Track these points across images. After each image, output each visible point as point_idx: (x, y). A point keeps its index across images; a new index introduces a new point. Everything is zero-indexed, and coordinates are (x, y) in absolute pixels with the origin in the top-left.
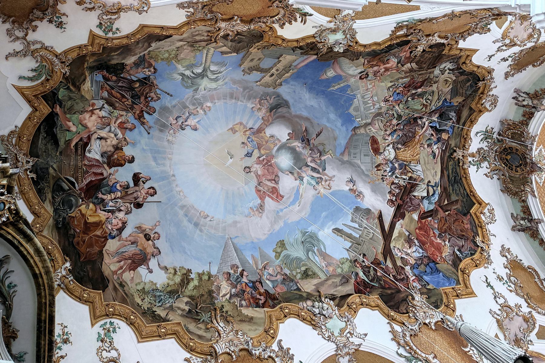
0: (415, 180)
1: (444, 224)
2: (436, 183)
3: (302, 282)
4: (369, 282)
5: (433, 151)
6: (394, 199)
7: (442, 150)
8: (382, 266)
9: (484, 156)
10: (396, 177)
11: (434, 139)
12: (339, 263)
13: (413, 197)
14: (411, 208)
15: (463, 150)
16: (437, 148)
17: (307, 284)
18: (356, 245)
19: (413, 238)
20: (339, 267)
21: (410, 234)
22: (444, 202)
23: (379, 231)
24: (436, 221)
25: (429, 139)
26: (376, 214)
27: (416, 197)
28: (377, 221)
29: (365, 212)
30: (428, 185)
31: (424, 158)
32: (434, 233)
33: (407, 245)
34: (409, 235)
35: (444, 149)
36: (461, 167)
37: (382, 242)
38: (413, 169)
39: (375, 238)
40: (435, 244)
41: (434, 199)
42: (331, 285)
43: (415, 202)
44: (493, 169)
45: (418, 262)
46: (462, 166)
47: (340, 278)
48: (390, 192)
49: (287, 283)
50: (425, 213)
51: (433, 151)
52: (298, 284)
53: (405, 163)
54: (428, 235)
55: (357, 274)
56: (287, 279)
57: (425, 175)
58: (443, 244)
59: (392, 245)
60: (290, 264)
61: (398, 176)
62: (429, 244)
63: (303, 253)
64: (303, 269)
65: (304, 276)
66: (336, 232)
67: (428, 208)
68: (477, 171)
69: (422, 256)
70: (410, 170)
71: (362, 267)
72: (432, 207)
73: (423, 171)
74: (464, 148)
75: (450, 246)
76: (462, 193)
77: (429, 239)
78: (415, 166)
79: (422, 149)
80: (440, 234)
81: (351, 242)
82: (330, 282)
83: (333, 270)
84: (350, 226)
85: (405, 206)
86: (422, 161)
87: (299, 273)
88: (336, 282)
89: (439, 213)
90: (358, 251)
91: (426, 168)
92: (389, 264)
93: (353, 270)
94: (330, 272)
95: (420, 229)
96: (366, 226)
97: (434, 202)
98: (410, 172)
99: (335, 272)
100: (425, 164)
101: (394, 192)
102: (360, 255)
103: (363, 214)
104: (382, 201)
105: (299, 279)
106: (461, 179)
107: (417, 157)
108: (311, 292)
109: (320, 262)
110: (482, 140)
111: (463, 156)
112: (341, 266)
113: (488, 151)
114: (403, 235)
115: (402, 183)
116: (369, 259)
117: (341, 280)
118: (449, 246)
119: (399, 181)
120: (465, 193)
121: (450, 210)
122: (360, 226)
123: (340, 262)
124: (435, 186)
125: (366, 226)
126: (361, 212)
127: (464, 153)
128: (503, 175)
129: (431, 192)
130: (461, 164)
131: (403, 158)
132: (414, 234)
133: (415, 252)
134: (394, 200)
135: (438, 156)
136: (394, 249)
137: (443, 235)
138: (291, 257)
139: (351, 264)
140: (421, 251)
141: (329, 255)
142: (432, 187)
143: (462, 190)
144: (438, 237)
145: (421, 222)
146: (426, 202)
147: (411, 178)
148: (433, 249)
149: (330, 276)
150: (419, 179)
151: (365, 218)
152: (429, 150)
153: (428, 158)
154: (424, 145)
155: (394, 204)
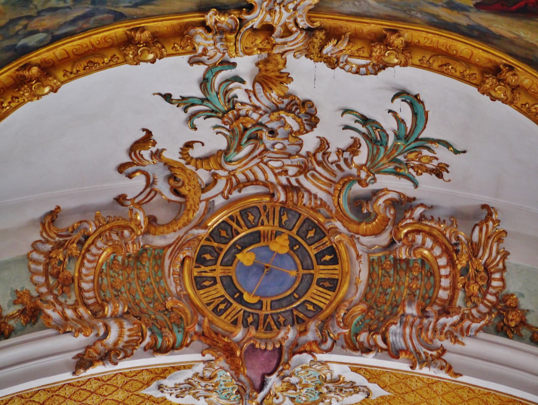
9: (265, 136)
15: (310, 32)
36: (197, 18)
44: (181, 176)
46: (203, 24)
68: (167, 97)
74: (321, 35)
76: (34, 24)
106: (119, 17)
110: (365, 120)
111: (268, 29)
113: (291, 149)
120: (31, 41)
127: (288, 32)
128: (152, 220)
130: (211, 18)
143: (47, 22)
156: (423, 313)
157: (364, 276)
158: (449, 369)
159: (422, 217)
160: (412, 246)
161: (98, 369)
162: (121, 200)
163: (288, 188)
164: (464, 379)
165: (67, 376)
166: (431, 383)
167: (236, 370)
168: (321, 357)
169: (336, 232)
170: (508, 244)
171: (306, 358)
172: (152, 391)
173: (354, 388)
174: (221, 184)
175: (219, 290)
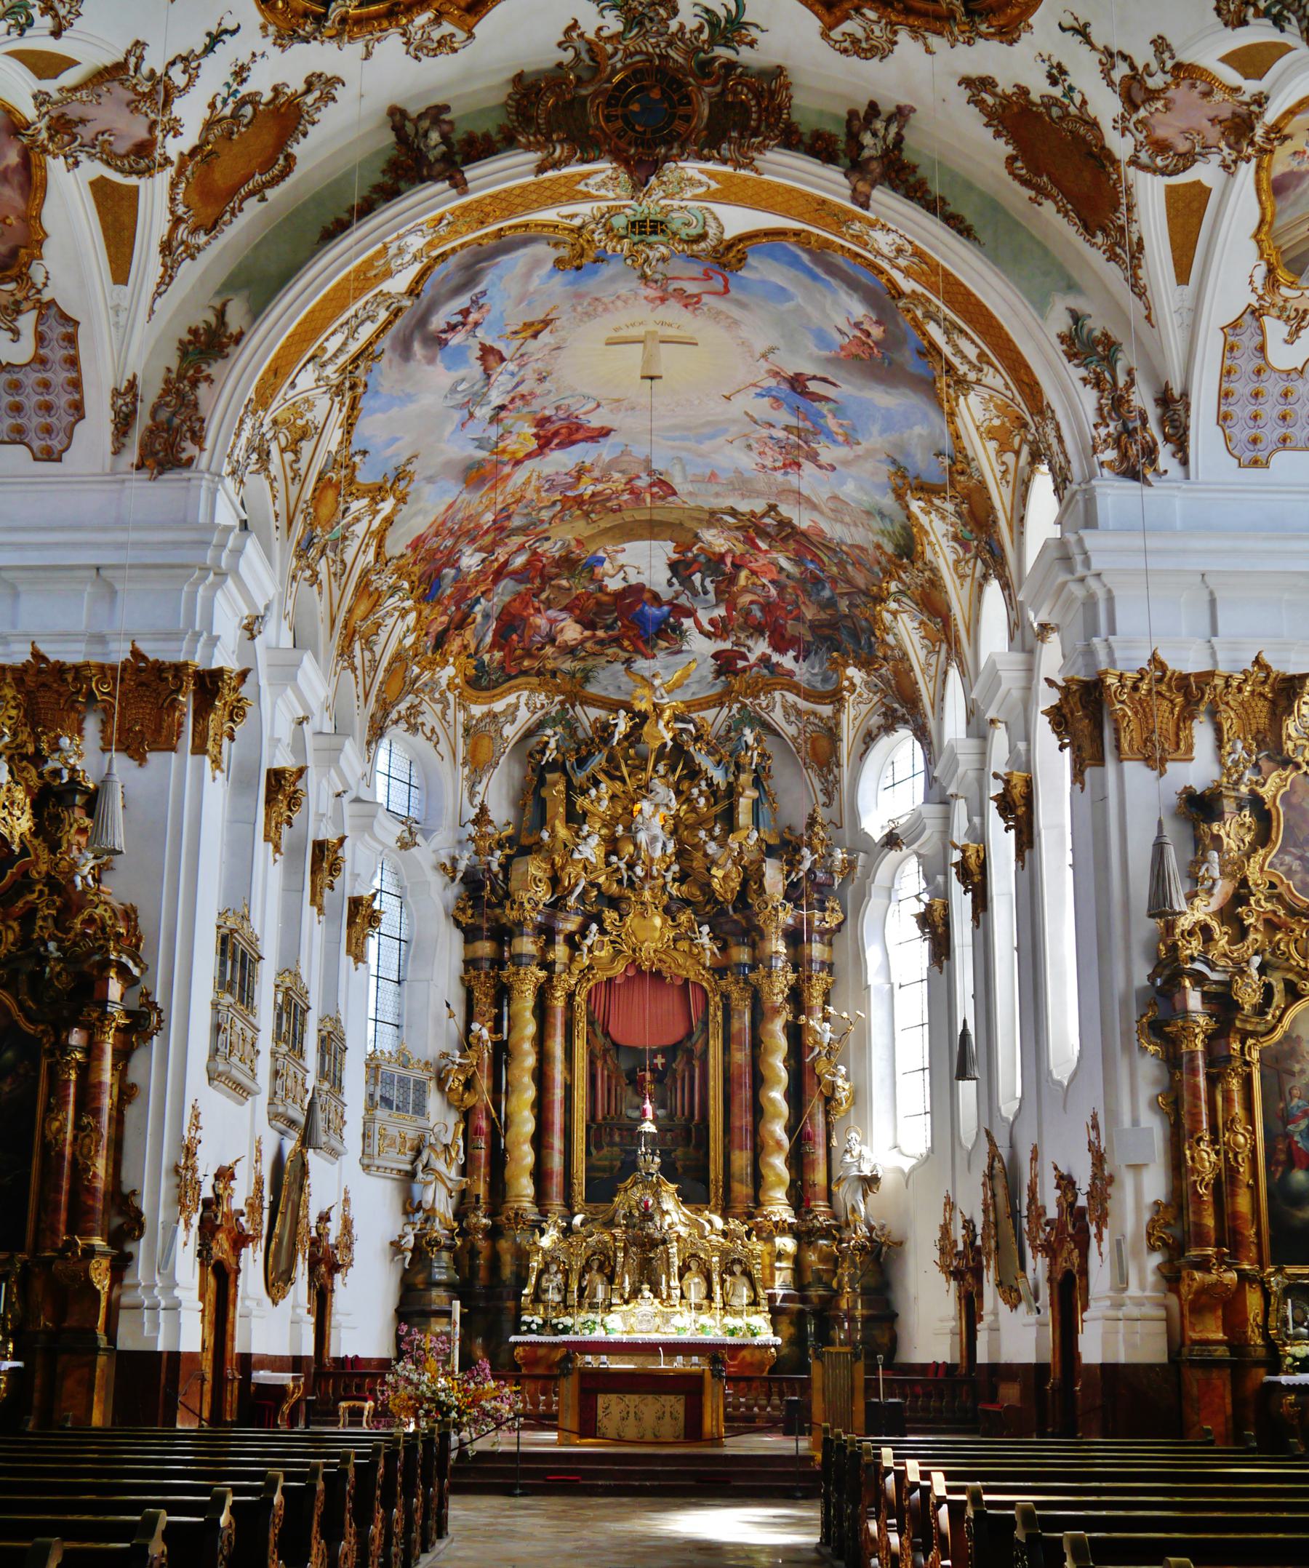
156: (742, 136)
157: (706, 113)
158: (756, 170)
159: (742, 74)
160: (736, 94)
161: (550, 174)
162: (560, 65)
163: (661, 56)
164: (766, 177)
165: (532, 178)
166: (745, 180)
167: (631, 174)
168: (681, 164)
169: (689, 84)
170: (793, 90)
171: (672, 165)
172: (581, 187)
173: (700, 184)
174: (620, 54)
175: (620, 124)
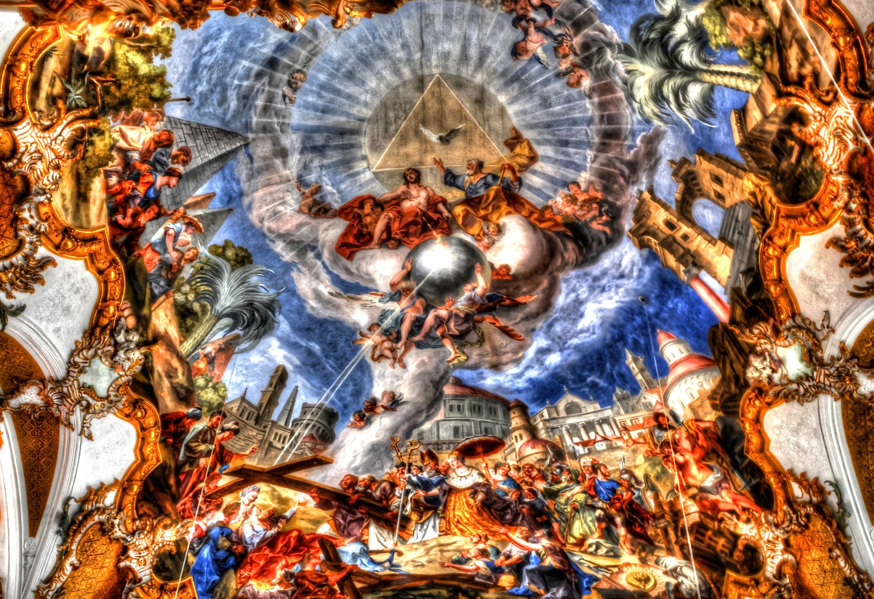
0: (403, 528)
1: (314, 583)
2: (399, 566)
3: (169, 306)
4: (185, 442)
5: (469, 559)
6: (361, 489)
7: (473, 577)
8: (219, 466)
10: (407, 492)
11: (499, 561)
12: (215, 380)
13: (365, 524)
14: (342, 521)
16: (478, 568)
17: (166, 316)
18: (255, 415)
19: (280, 525)
20: (208, 381)
21: (288, 520)
22: (360, 582)
23: (289, 459)
24: (317, 567)
25: (498, 553)
26: (326, 454)
27: (366, 531)
28: (309, 455)
29: (326, 431)
30: (392, 552)
31: (454, 543)
32: (293, 564)
33: (264, 513)
34: (284, 517)
35: (477, 579)
37: (266, 466)
38: (427, 523)
39: (273, 453)
40: (273, 566)
41: (362, 563)
42: (170, 365)
43: (357, 532)
45: (234, 536)
47: (186, 384)
48: (373, 480)
49: (163, 273)
50: (334, 547)
51: (469, 559)
52: (163, 297)
53: (441, 508)
54: (287, 554)
55: (197, 418)
56: (171, 271)
57: (415, 546)
58: (274, 581)
59: (263, 486)
60: (203, 280)
61: (411, 495)
62: (271, 555)
63: (228, 304)
64: (196, 307)
65: (182, 310)
66: (279, 373)
67: (344, 552)
69: (246, 543)
70: (424, 518)
71: (212, 428)
72: (347, 560)
73: (423, 543)
75: (270, 594)
77: (280, 555)
78: (434, 527)
79: (475, 539)
80: (292, 575)
81: (261, 405)
82: (175, 363)
83: (199, 370)
84: (293, 402)
85: (344, 509)
86: (444, 540)
87: (187, 299)
88: (177, 377)
89: (333, 573)
90: (244, 418)
91: (432, 548)
92: (224, 481)
93: (205, 409)
94: (195, 364)
95: (300, 538)
96: (296, 433)
97: (358, 563)
98: (421, 517)
99: (196, 374)
100: (441, 545)
101: (374, 488)
102: (237, 424)
103: (322, 428)
104: (353, 466)
105: (175, 300)
107: (456, 530)
108: (152, 326)
109: (213, 343)
112: (210, 384)
114: (283, 507)
115: (396, 502)
116: (230, 442)
117: (182, 386)
118: (272, 591)
119: (399, 498)
121: (342, 593)
122: (296, 423)
123: (217, 383)
124: (392, 565)
125: (296, 433)
126: (325, 423)
129: (377, 558)
131: (452, 504)
132: (288, 528)
133: (253, 529)
134: (357, 488)
135: (459, 569)
136: (254, 490)
137: (292, 581)
138: (217, 281)
139: (216, 405)
140: (256, 540)
141: (228, 359)
142: (390, 560)
144: (287, 573)
145: (313, 540)
146: (356, 548)
147: (406, 520)
148: (262, 563)
149: (187, 363)
150: (405, 535)
151: (314, 432)
152: (473, 552)
153: (454, 551)
154: (485, 543)
155: (348, 488)
